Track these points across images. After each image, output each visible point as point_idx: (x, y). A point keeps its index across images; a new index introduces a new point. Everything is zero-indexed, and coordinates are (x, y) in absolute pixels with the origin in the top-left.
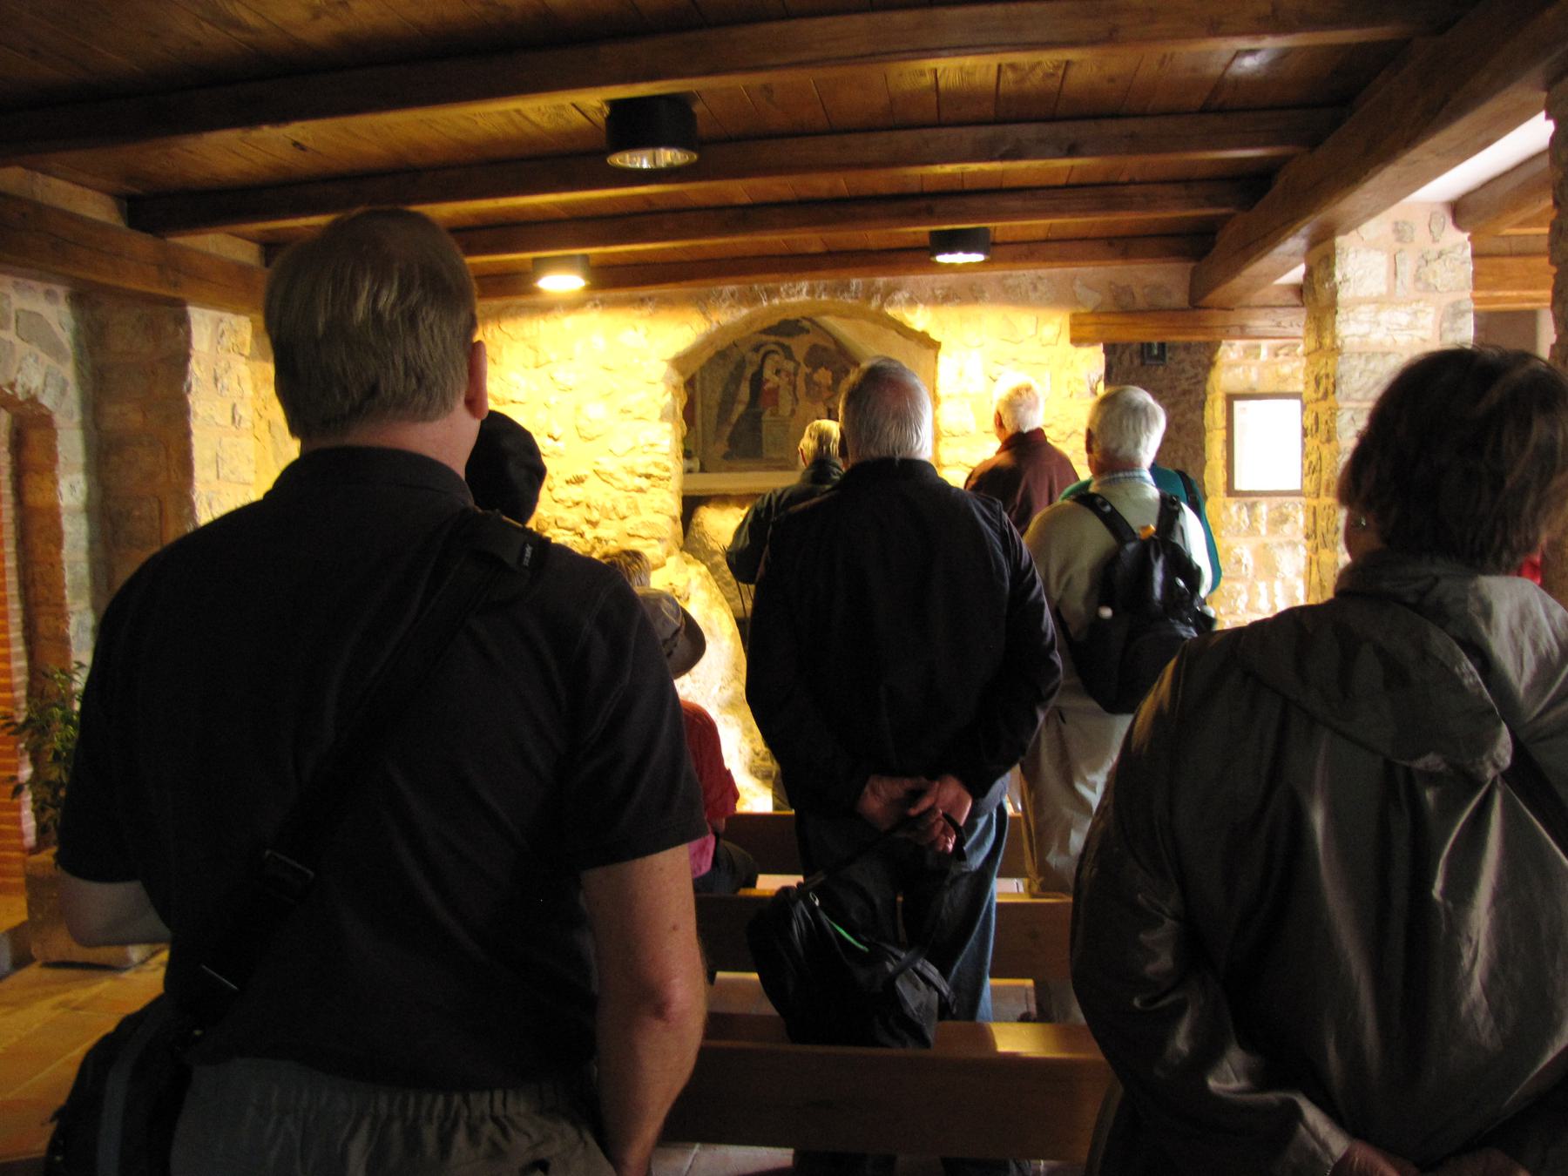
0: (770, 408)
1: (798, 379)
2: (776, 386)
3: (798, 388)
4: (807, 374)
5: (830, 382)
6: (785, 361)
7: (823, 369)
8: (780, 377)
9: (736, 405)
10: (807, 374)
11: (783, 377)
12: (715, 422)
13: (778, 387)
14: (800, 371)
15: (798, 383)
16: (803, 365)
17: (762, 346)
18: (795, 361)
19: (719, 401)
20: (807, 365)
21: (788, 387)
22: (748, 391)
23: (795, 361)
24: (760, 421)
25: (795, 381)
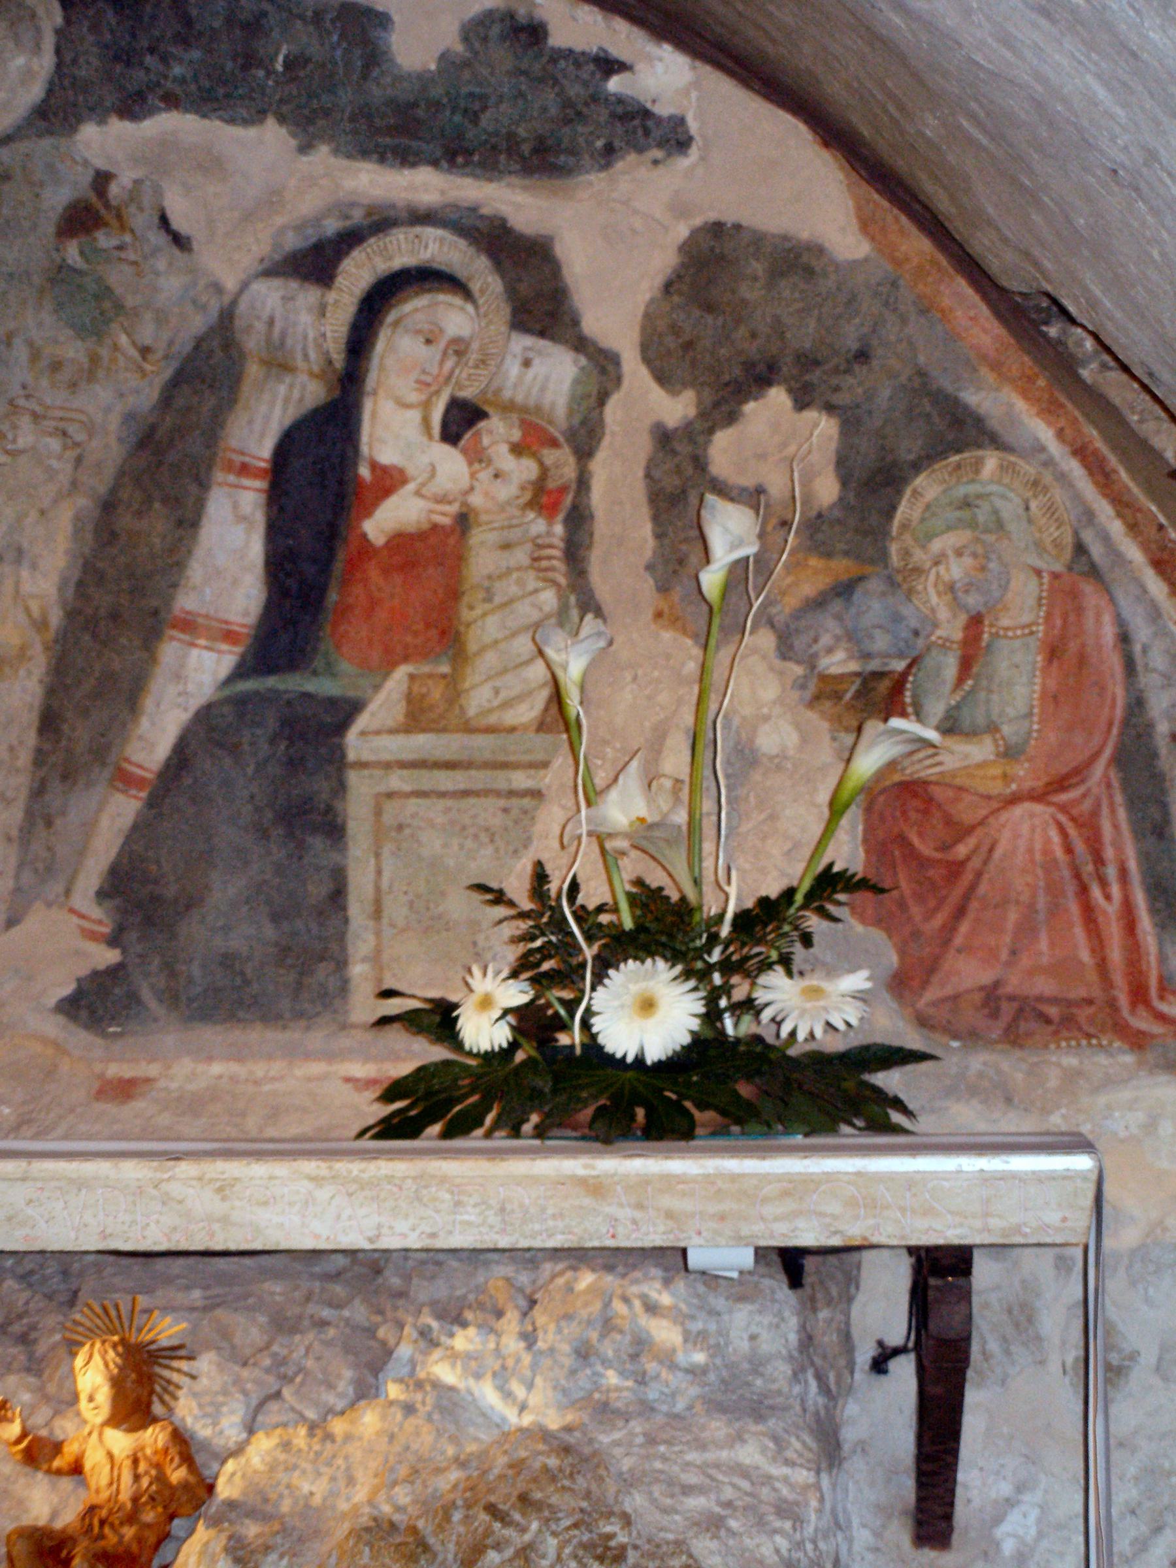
0: (401, 672)
1: (601, 468)
2: (444, 516)
3: (602, 527)
4: (664, 438)
5: (827, 490)
6: (521, 343)
7: (778, 397)
8: (477, 457)
9: (169, 650)
10: (664, 438)
11: (505, 460)
12: (25, 758)
13: (464, 521)
14: (613, 411)
15: (597, 496)
16: (634, 369)
17: (350, 239)
18: (581, 344)
19: (56, 618)
20: (662, 378)
21: (538, 526)
22: (256, 549)
23: (581, 344)
24: (337, 761)
25: (583, 483)
